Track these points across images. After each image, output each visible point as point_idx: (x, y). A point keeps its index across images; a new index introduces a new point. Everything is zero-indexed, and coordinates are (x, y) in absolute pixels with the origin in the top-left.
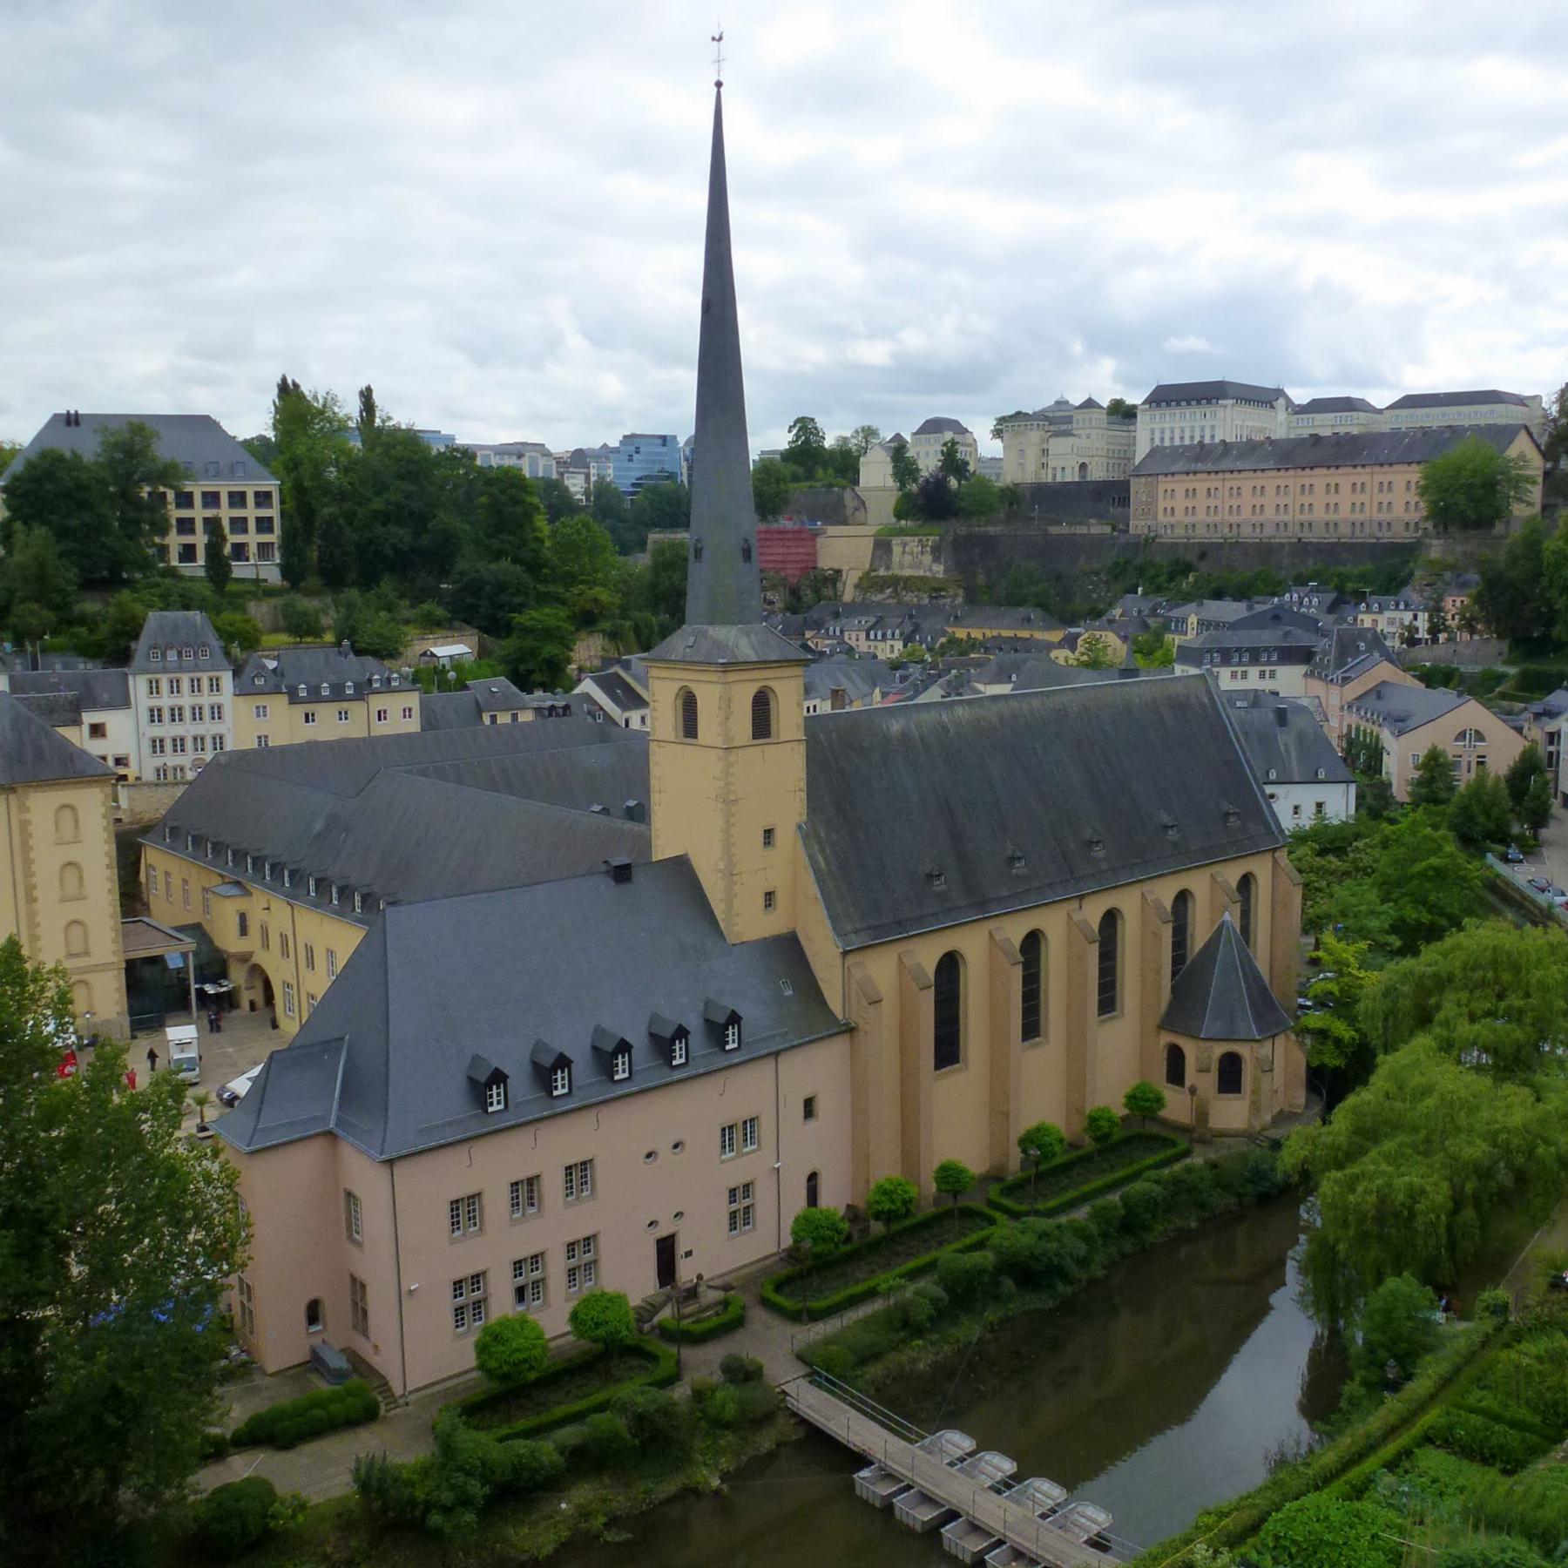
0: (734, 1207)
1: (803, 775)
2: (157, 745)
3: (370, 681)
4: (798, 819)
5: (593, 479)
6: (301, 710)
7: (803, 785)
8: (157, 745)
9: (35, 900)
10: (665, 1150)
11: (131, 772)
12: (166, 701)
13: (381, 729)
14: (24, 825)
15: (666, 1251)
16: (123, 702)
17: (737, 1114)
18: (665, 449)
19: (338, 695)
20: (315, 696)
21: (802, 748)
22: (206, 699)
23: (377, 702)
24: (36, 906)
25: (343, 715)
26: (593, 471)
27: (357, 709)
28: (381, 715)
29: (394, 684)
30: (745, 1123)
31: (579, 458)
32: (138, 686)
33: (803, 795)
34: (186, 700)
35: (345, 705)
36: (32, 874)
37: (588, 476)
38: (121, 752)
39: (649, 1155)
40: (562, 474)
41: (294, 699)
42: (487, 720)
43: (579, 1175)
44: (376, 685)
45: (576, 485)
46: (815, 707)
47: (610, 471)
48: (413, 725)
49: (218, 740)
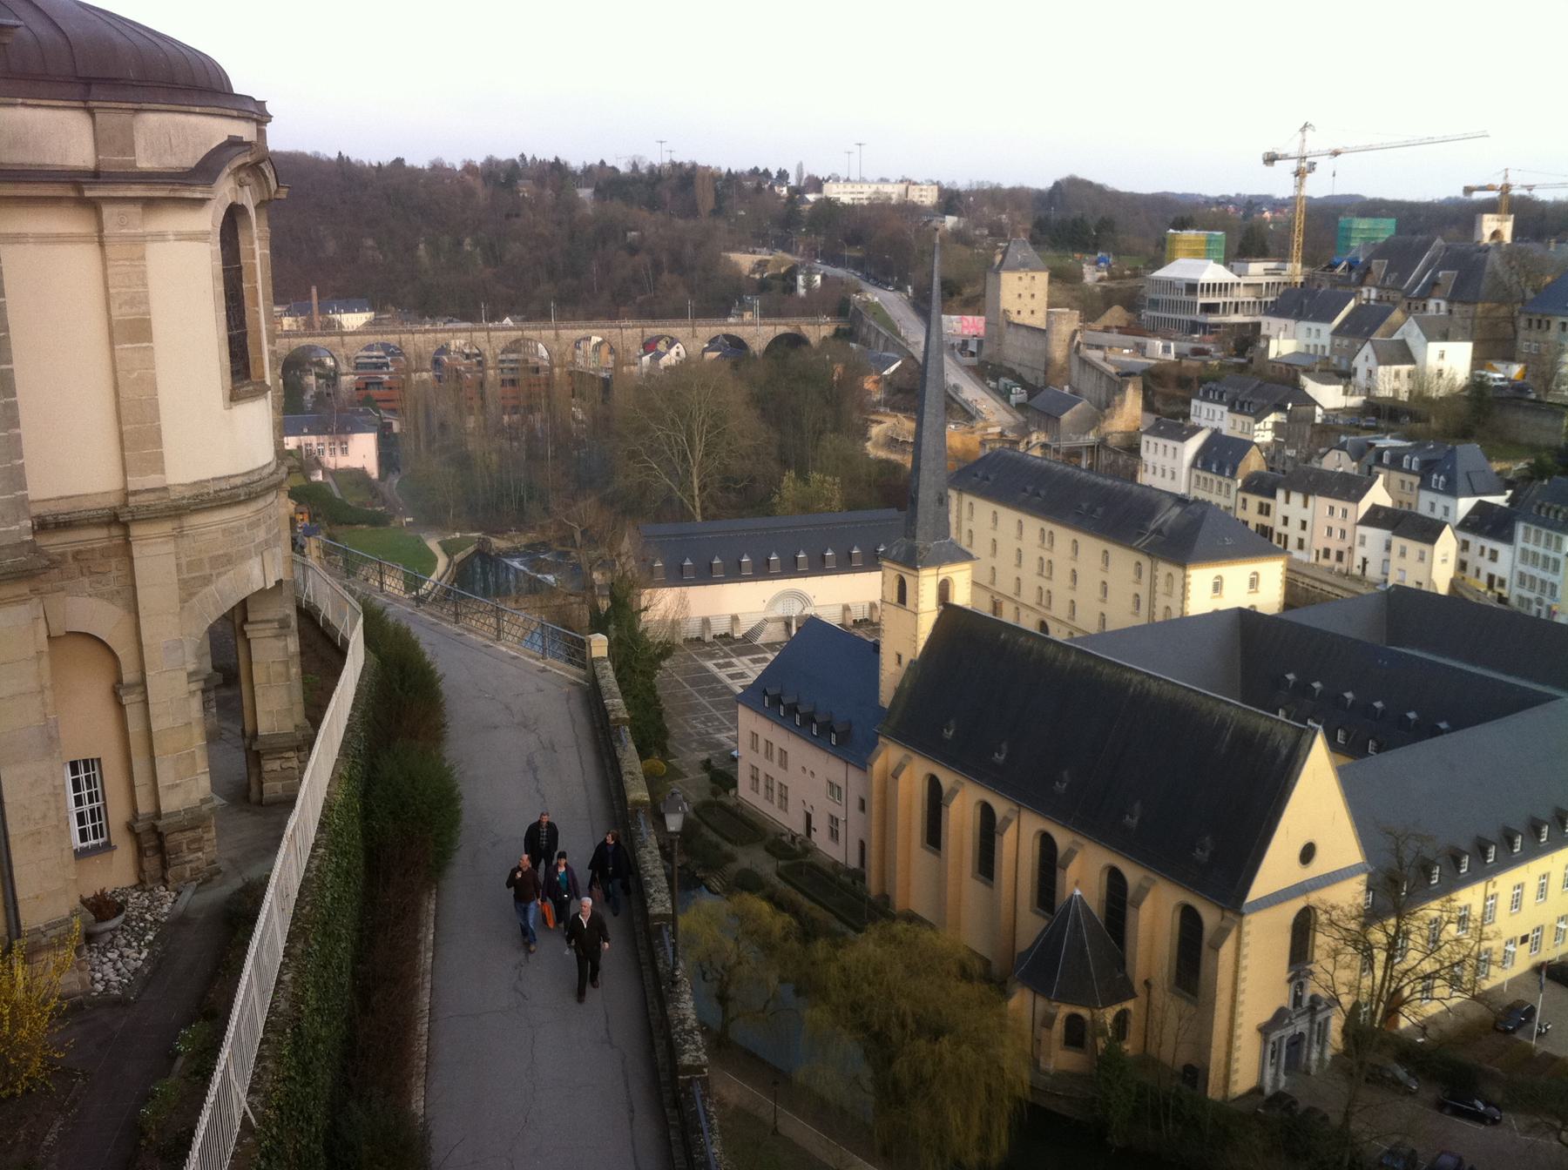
2: (1522, 576)
8: (1522, 576)
11: (1505, 593)
12: (1531, 547)
14: (1156, 577)
16: (1508, 539)
22: (1552, 554)
32: (1520, 528)
34: (1541, 550)
36: (1154, 606)
49: (1554, 586)
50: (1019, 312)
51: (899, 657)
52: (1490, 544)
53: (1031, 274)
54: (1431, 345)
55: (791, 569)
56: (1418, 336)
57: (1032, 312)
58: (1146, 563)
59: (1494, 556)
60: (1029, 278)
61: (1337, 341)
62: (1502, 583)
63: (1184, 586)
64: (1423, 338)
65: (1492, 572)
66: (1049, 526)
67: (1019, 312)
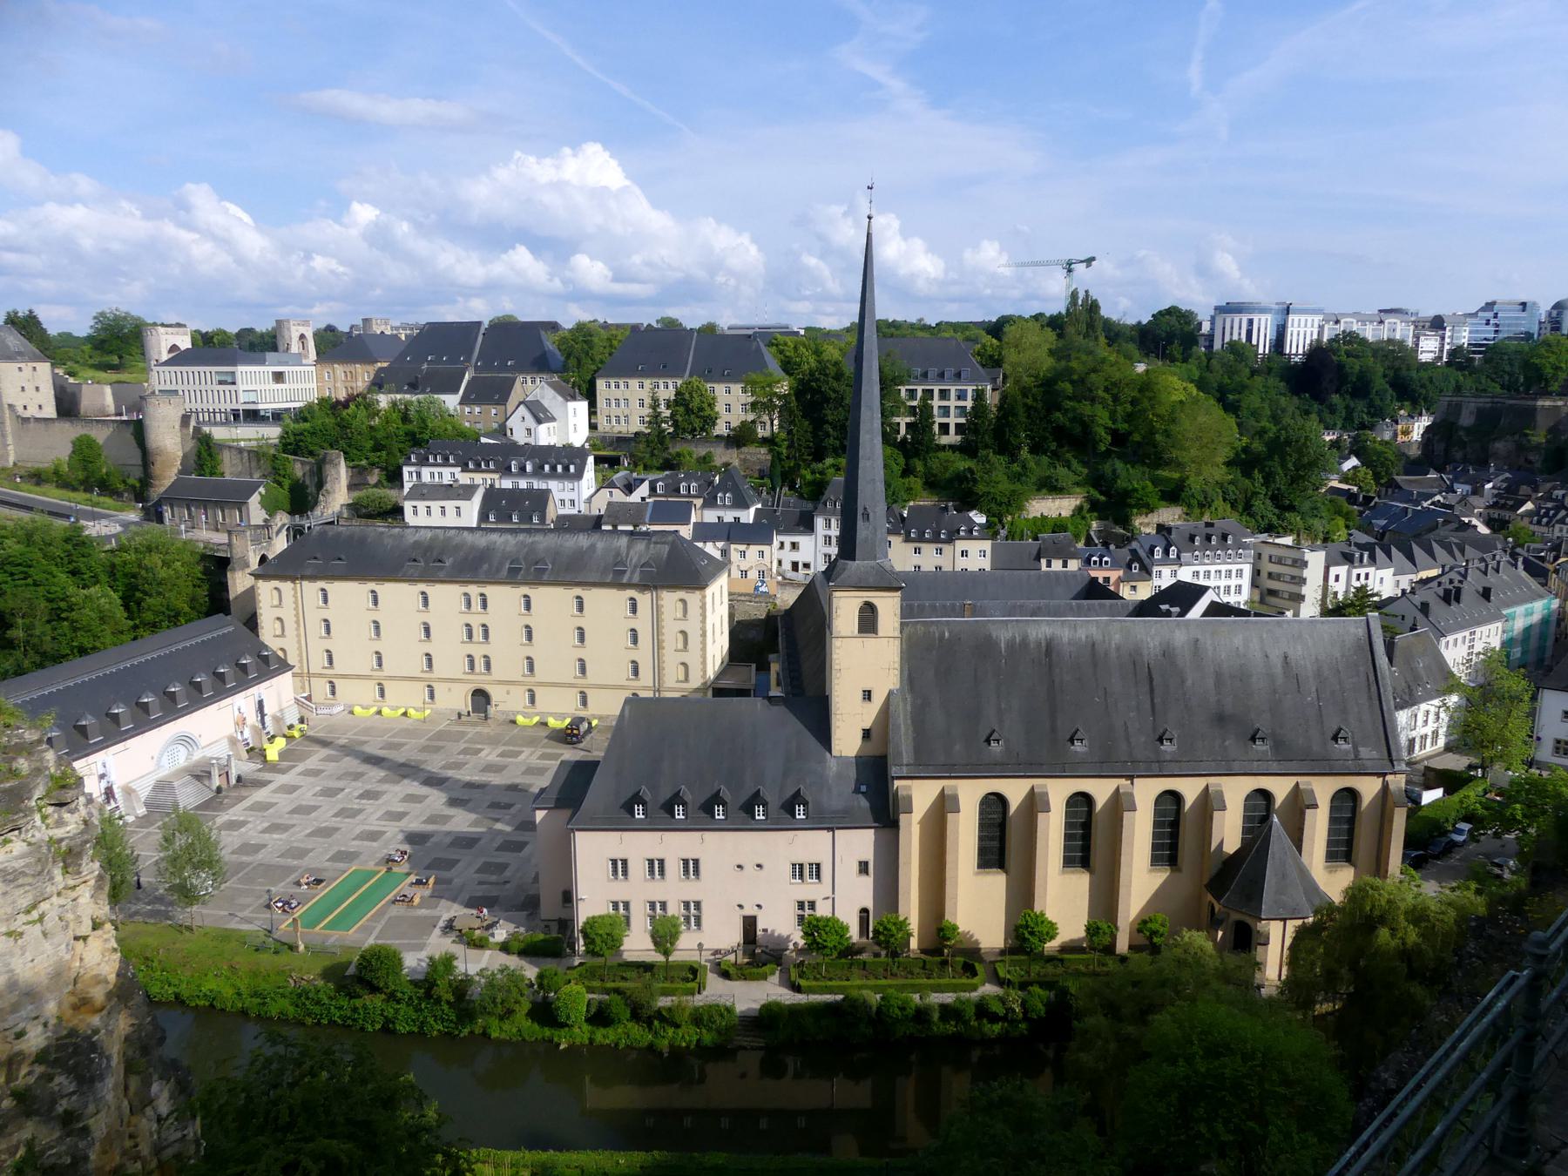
0: (800, 912)
1: (897, 659)
3: (958, 531)
4: (892, 687)
5: (1447, 340)
6: (912, 546)
7: (897, 665)
9: (663, 648)
10: (750, 868)
13: (962, 563)
15: (750, 924)
17: (806, 858)
18: (1523, 314)
19: (936, 539)
20: (921, 539)
21: (897, 642)
23: (961, 545)
24: (664, 651)
25: (940, 551)
26: (1448, 334)
27: (947, 548)
28: (964, 553)
29: (975, 533)
30: (811, 864)
31: (1437, 324)
33: (897, 673)
35: (940, 546)
37: (1443, 338)
38: (807, 560)
39: (739, 866)
40: (1417, 337)
41: (908, 539)
42: (1044, 562)
43: (692, 867)
44: (962, 533)
45: (1429, 348)
46: (1367, 575)
47: (1466, 334)
48: (986, 564)
50: (25, 407)
51: (868, 695)
52: (788, 540)
53: (31, 365)
54: (569, 403)
55: (172, 709)
56: (554, 397)
57: (40, 407)
58: (644, 600)
59: (794, 546)
60: (31, 369)
61: (467, 409)
62: (807, 566)
63: (703, 607)
64: (560, 399)
65: (795, 560)
66: (473, 590)
67: (25, 407)
